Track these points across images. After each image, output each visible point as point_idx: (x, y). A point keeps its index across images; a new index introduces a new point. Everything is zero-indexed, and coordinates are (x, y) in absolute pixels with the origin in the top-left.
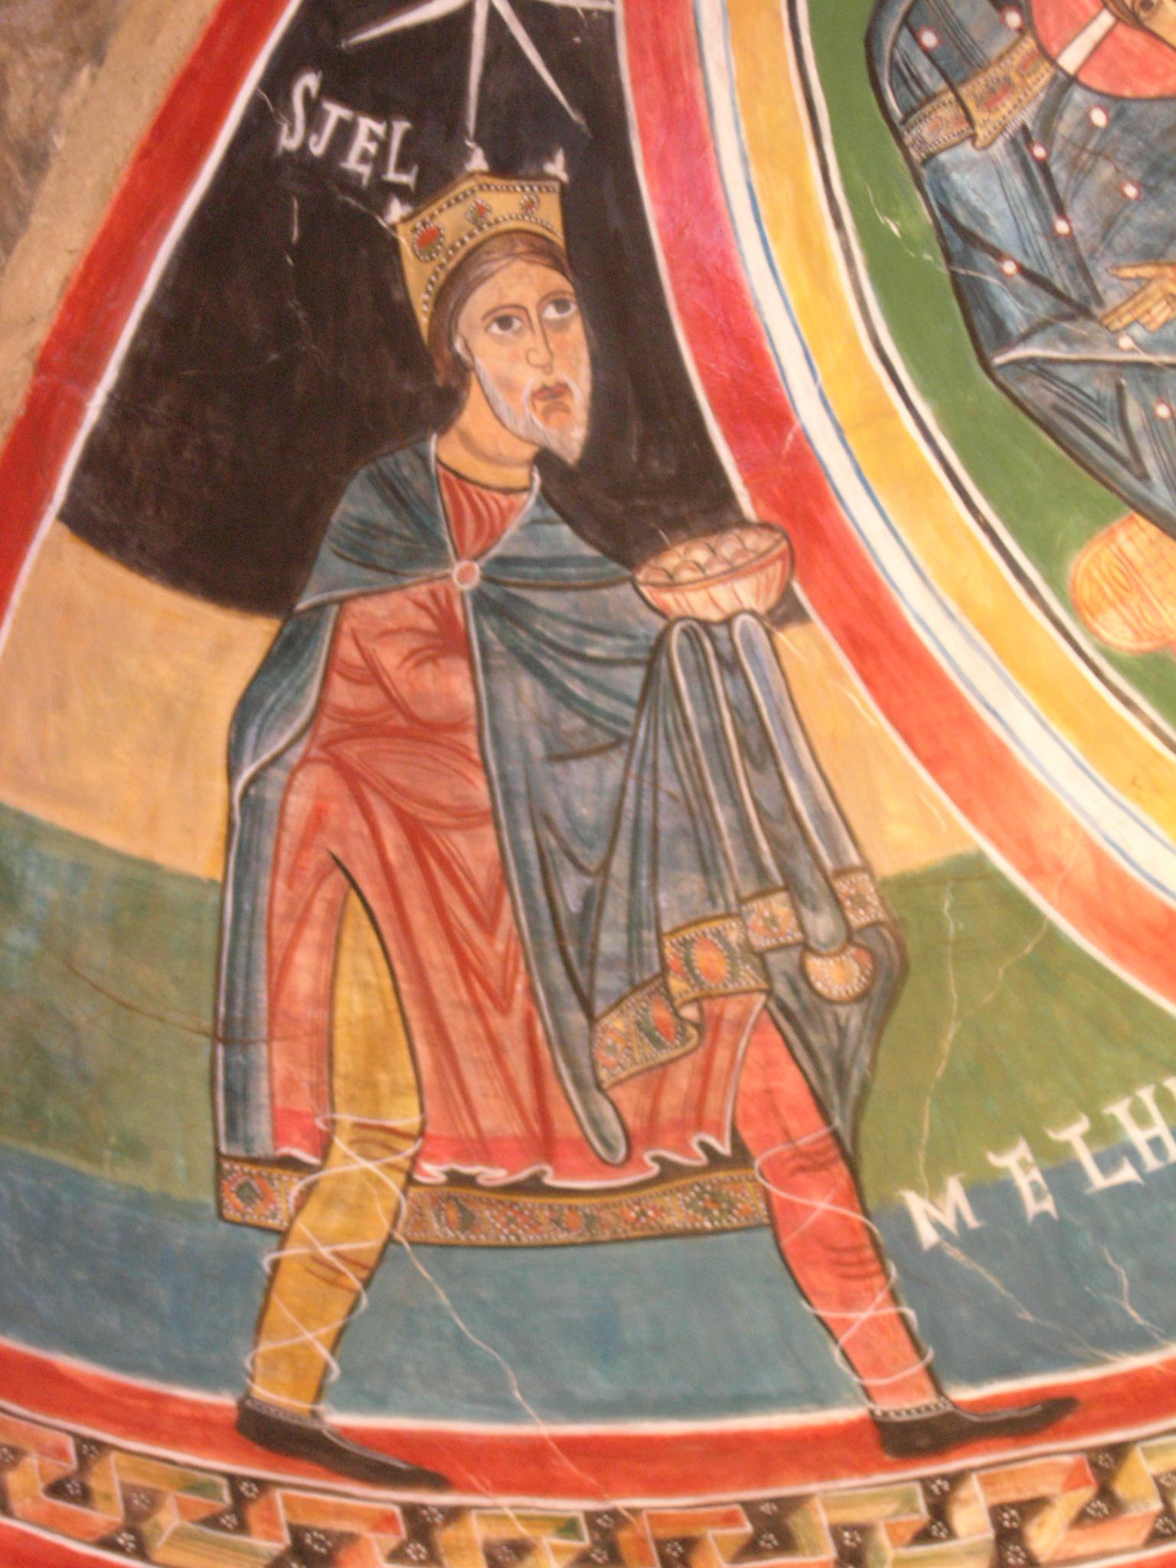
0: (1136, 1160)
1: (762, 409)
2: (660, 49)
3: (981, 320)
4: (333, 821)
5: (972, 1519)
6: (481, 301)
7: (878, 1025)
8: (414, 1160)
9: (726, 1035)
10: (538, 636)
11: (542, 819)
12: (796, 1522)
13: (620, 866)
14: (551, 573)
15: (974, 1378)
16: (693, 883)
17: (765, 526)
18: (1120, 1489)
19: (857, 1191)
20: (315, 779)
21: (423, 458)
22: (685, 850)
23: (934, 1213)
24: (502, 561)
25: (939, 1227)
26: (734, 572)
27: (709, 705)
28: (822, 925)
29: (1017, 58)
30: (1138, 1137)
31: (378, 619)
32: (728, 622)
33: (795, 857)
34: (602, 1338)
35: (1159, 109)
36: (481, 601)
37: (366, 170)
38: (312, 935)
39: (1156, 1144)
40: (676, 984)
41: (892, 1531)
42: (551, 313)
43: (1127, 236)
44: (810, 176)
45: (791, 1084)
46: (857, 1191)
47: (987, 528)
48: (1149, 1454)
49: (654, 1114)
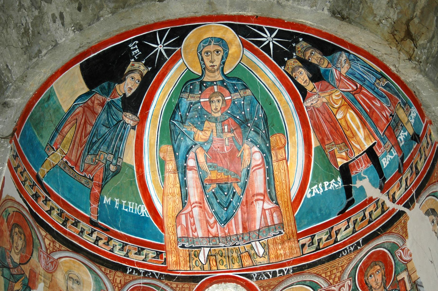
0: (128, 210)
1: (147, 107)
2: (168, 67)
3: (173, 116)
4: (79, 115)
5: (95, 236)
6: (132, 75)
7: (113, 176)
8: (64, 157)
9: (98, 166)
10: (110, 111)
12: (78, 224)
13: (101, 140)
14: (116, 106)
15: (101, 221)
16: (106, 148)
17: (138, 118)
18: (109, 243)
19: (100, 192)
20: (81, 109)
21: (114, 85)
22: (107, 144)
23: (107, 200)
24: (113, 101)
25: (106, 202)
26: (132, 120)
27: (120, 131)
28: (114, 162)
29: (197, 96)
30: (130, 207)
31: (99, 97)
32: (128, 124)
33: (117, 153)
34: (70, 190)
35: (205, 112)
36: (108, 102)
37: (134, 54)
38: (70, 125)
39: (131, 209)
40: (97, 157)
41: (87, 232)
42: (137, 81)
43: (192, 120)
44: (170, 90)
46: (100, 192)
47: (158, 135)
48: (114, 241)
49: (87, 169)
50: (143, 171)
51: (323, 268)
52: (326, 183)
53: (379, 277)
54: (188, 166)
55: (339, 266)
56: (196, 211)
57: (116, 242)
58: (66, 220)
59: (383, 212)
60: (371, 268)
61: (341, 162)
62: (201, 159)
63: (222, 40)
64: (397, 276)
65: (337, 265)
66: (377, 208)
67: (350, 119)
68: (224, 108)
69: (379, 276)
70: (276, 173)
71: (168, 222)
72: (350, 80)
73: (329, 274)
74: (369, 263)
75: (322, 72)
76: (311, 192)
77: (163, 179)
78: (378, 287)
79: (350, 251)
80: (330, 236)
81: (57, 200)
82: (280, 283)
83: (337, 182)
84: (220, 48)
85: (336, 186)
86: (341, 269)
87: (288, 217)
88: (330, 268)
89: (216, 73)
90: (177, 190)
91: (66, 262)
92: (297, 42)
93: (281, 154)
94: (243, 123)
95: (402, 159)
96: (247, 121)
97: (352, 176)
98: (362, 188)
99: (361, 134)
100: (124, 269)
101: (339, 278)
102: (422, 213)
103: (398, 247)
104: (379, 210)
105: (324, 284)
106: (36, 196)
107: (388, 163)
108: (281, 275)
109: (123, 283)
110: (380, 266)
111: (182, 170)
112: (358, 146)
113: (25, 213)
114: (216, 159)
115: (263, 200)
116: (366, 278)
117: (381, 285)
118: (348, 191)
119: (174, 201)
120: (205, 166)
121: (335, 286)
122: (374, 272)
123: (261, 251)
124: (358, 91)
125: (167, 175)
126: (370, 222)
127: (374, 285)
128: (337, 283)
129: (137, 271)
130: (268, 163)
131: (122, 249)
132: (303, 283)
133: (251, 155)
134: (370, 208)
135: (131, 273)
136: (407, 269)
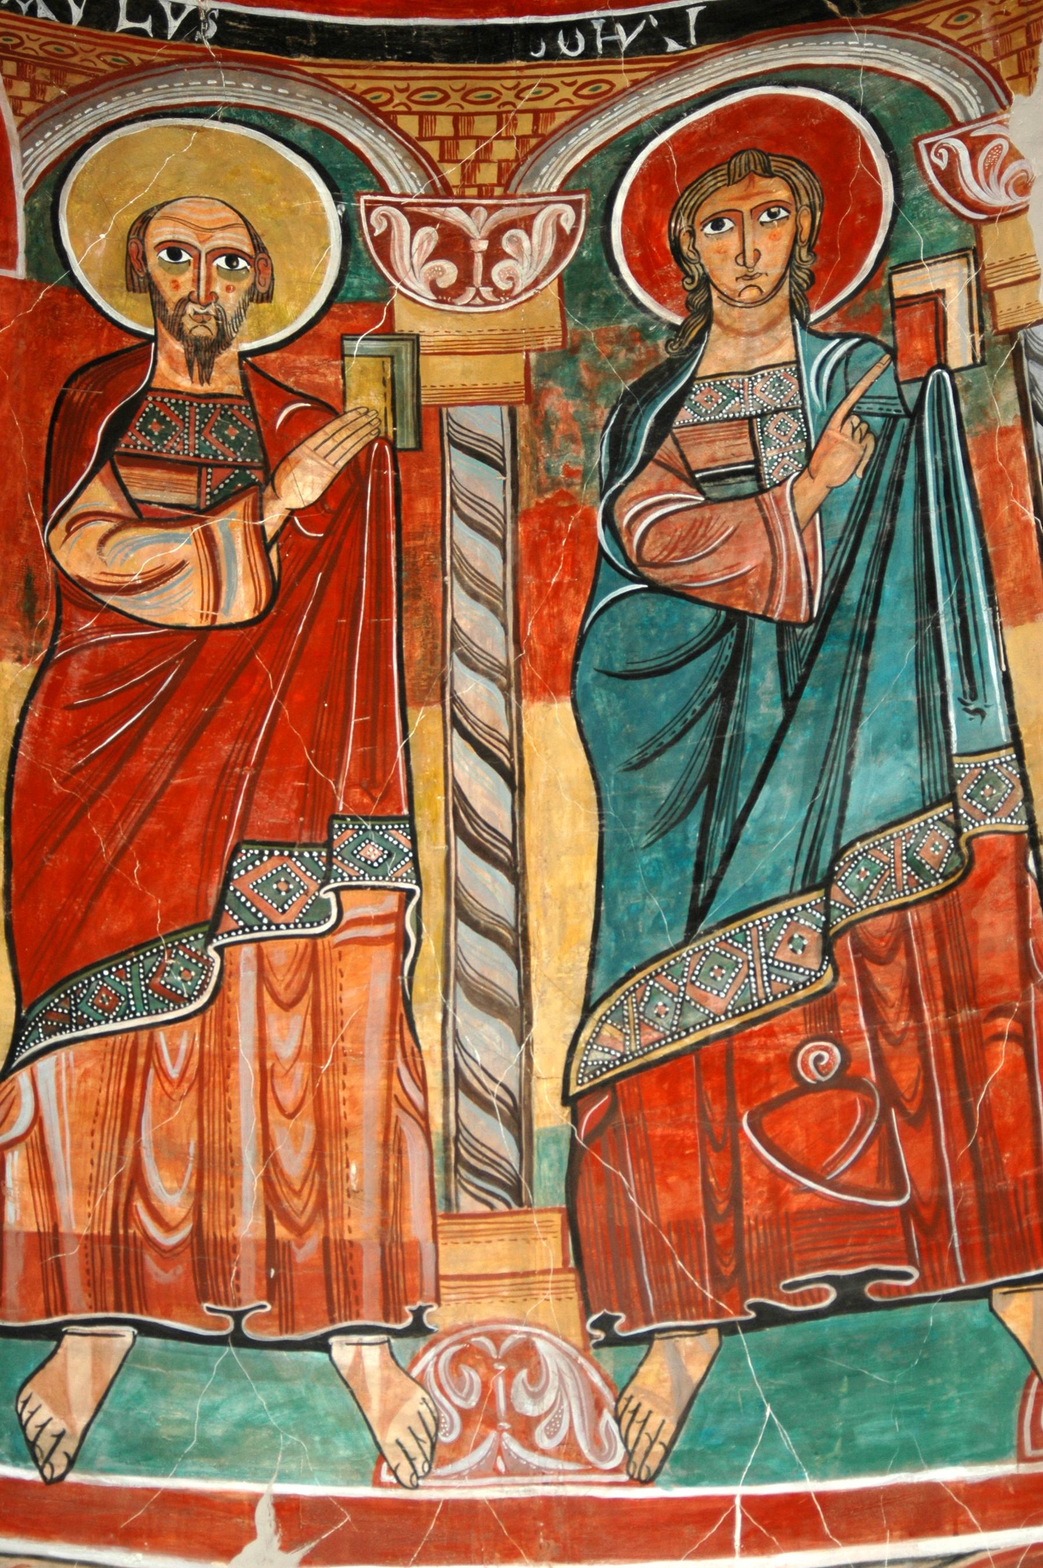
51: (415, 85)
53: (772, 248)
55: (521, 105)
60: (731, 181)
64: (897, 269)
65: (508, 96)
69: (774, 237)
73: (444, 127)
74: (724, 149)
78: (749, 295)
79: (612, 47)
86: (525, 125)
88: (455, 97)
101: (507, 173)
103: (946, 119)
105: (404, 176)
108: (142, 32)
110: (794, 190)
116: (684, 224)
117: (777, 288)
121: (468, 209)
122: (746, 207)
127: (727, 275)
128: (484, 191)
132: (276, 125)
136: (978, 253)
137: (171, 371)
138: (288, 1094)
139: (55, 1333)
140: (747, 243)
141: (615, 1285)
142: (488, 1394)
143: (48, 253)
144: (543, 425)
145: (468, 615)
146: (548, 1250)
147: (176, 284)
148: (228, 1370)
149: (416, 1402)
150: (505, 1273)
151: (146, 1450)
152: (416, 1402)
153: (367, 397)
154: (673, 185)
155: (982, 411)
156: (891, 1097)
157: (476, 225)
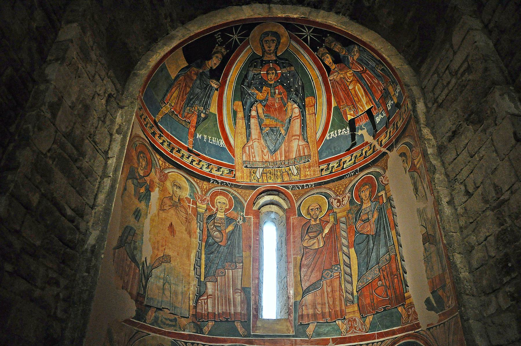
5: (190, 159)
6: (216, 55)
11: (193, 91)
14: (206, 75)
23: (199, 136)
33: (206, 106)
44: (241, 65)
45: (196, 120)
50: (222, 118)
52: (339, 131)
53: (367, 193)
54: (251, 115)
56: (256, 144)
57: (204, 163)
58: (173, 149)
59: (374, 152)
61: (350, 118)
62: (260, 111)
63: (276, 33)
66: (370, 149)
67: (358, 89)
68: (277, 78)
70: (308, 122)
71: (238, 151)
72: (359, 64)
73: (337, 189)
75: (341, 57)
76: (330, 136)
77: (235, 124)
80: (340, 165)
81: (167, 136)
82: (306, 193)
83: (346, 130)
84: (274, 38)
85: (346, 133)
87: (314, 151)
89: (272, 55)
90: (244, 131)
91: (172, 175)
92: (326, 36)
93: (312, 110)
94: (288, 89)
95: (389, 118)
96: (291, 87)
97: (357, 127)
98: (362, 135)
99: (364, 100)
100: (208, 180)
102: (398, 154)
104: (372, 150)
106: (154, 134)
107: (379, 120)
109: (208, 189)
111: (248, 118)
112: (362, 108)
113: (147, 145)
114: (270, 111)
115: (299, 139)
118: (353, 136)
119: (242, 138)
120: (262, 116)
123: (295, 172)
124: (364, 72)
125: (238, 120)
126: (365, 157)
127: (364, 198)
129: (217, 182)
130: (303, 116)
131: (208, 168)
132: (321, 193)
133: (292, 109)
134: (366, 148)
135: (213, 183)
137: (313, 223)
138: (330, 296)
139: (309, 324)
140: (365, 194)
141: (363, 312)
142: (352, 325)
143: (300, 215)
144: (349, 218)
145: (344, 241)
146: (356, 308)
147: (312, 213)
148: (326, 326)
149: (345, 327)
150: (352, 311)
151: (319, 335)
152: (345, 327)
153: (332, 219)
154: (358, 189)
155: (387, 207)
156: (387, 287)
157: (340, 198)
